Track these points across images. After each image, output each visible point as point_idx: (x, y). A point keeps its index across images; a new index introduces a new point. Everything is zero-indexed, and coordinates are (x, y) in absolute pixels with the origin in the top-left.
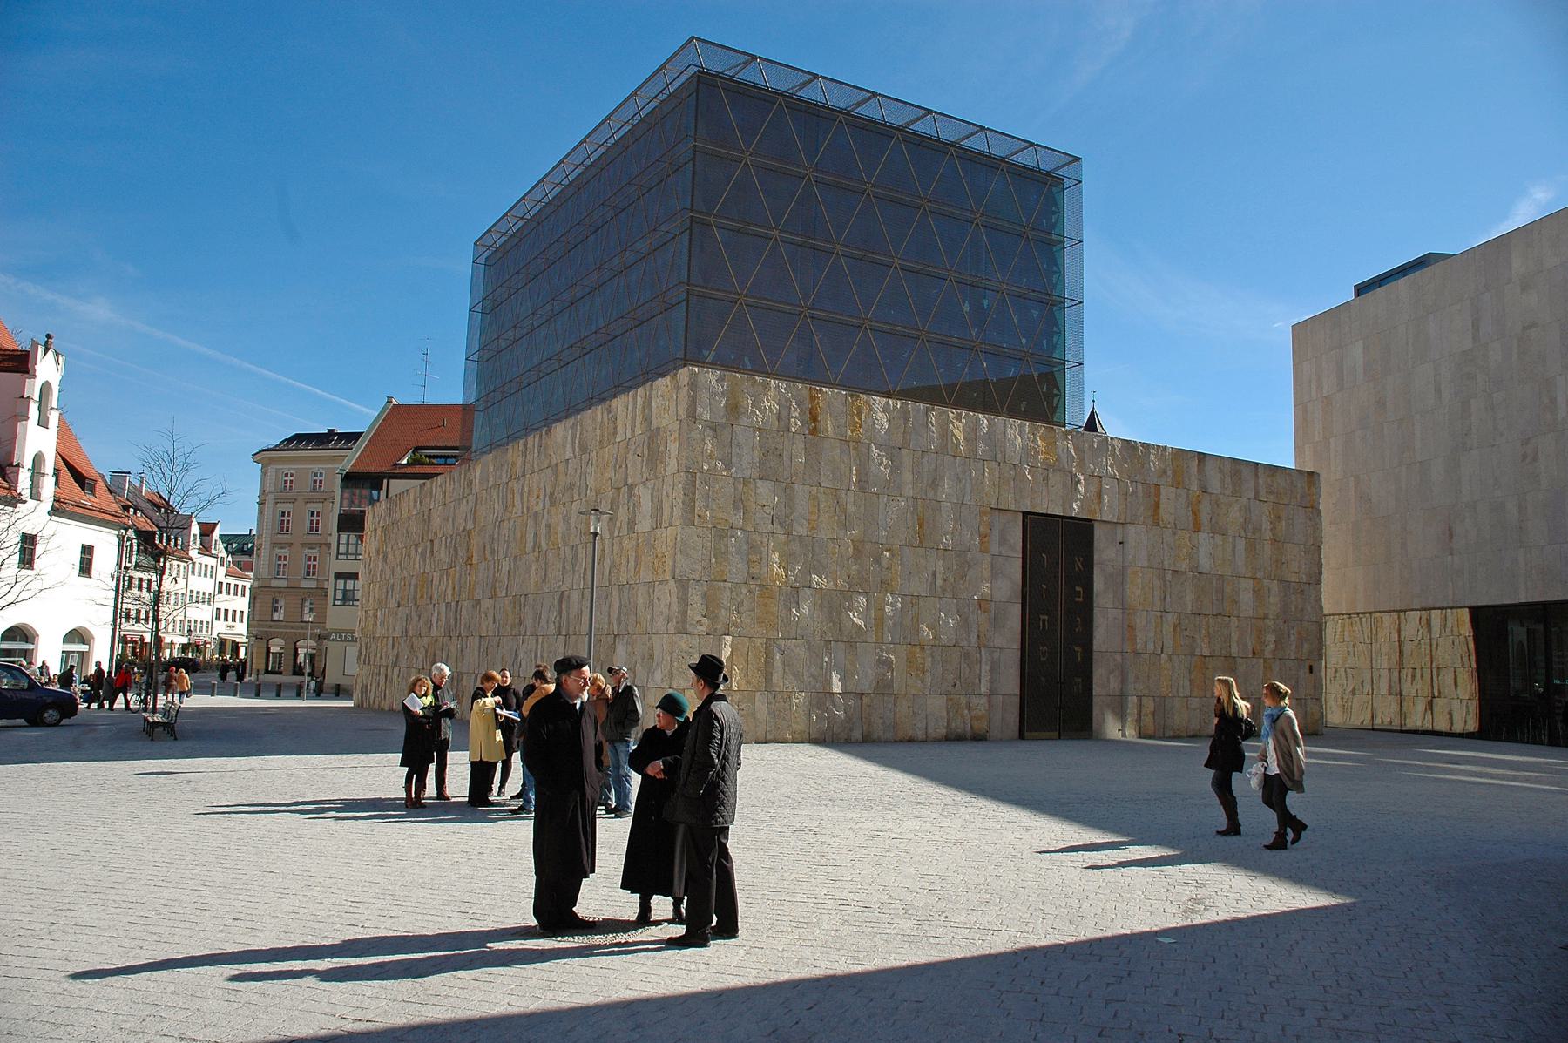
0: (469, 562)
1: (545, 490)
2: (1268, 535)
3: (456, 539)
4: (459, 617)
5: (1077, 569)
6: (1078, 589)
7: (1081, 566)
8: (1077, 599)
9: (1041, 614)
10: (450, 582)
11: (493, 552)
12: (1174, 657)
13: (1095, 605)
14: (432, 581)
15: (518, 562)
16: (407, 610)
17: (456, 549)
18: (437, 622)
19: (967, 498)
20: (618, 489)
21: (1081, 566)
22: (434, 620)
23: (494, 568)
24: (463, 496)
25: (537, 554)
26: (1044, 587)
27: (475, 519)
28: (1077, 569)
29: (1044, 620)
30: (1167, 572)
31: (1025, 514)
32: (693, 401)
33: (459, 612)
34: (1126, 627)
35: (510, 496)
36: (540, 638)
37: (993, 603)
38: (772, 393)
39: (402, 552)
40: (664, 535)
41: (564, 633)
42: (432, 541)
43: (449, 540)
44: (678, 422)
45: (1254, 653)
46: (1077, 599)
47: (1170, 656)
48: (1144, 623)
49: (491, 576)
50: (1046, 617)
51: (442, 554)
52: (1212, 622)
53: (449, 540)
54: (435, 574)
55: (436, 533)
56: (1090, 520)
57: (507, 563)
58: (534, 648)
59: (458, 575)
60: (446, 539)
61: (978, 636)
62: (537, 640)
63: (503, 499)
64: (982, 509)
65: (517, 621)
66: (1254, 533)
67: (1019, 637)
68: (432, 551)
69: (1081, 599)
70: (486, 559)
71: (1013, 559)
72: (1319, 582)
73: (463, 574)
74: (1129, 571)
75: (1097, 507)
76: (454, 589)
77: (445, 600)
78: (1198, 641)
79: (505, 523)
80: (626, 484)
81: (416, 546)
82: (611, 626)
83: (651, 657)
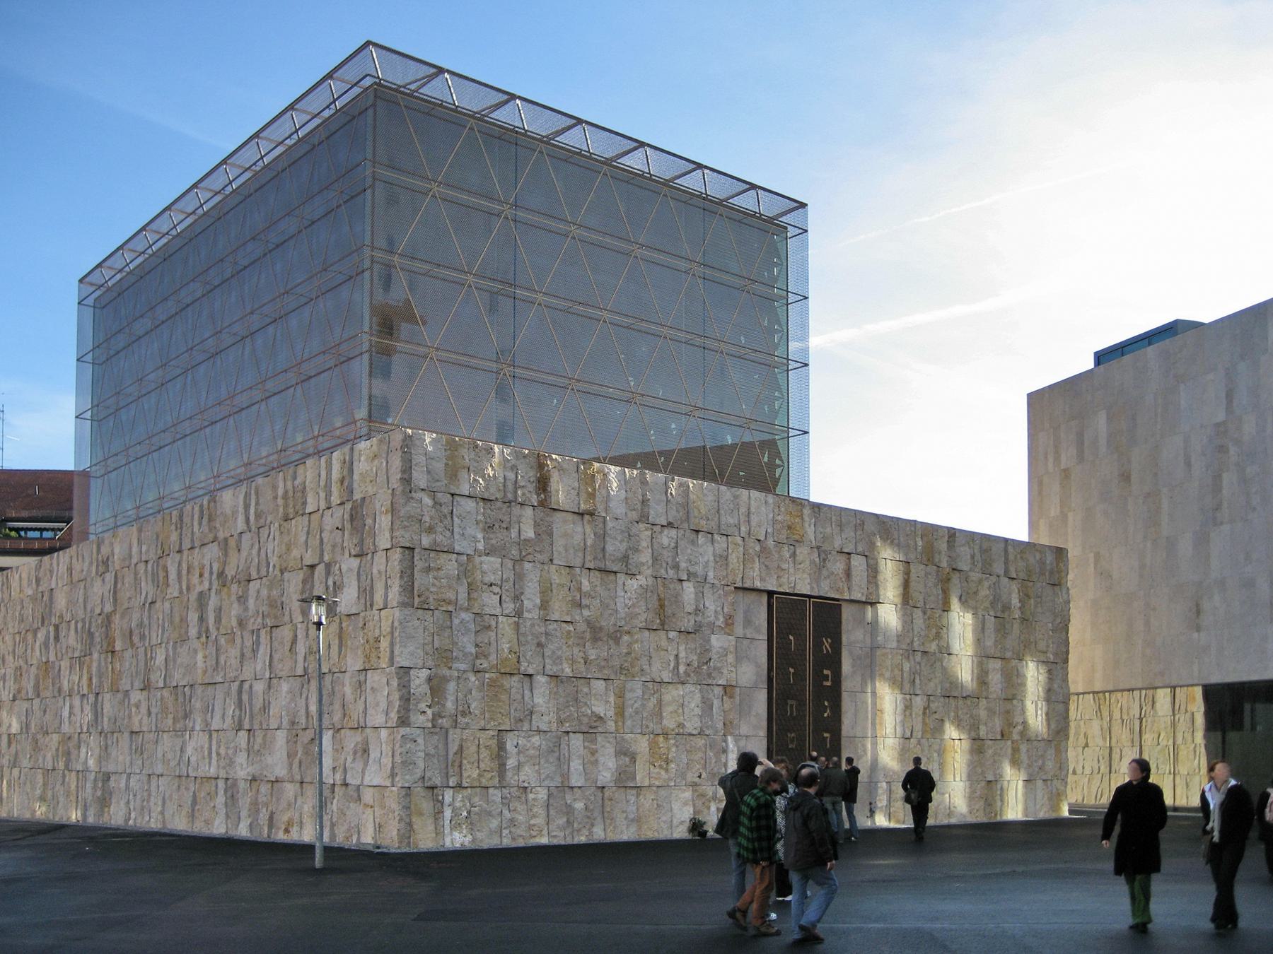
0: (110, 648)
1: (211, 568)
2: (1017, 614)
3: (90, 623)
4: (99, 710)
6: (826, 672)
7: (830, 650)
9: (788, 698)
10: (85, 672)
11: (143, 637)
12: (924, 741)
13: (843, 688)
14: (60, 670)
15: (179, 649)
16: (26, 705)
17: (91, 635)
18: (70, 717)
19: (711, 574)
20: (312, 567)
21: (830, 650)
22: (66, 713)
23: (146, 655)
24: (97, 573)
25: (203, 639)
26: (792, 670)
27: (115, 600)
31: (770, 594)
32: (407, 469)
33: (99, 704)
35: (162, 574)
36: (215, 735)
37: (738, 689)
38: (496, 460)
39: (14, 638)
40: (376, 618)
41: (247, 726)
42: (57, 627)
43: (80, 625)
44: (390, 491)
45: (1002, 736)
47: (919, 743)
49: (142, 664)
50: (794, 702)
51: (71, 639)
52: (961, 702)
53: (80, 625)
54: (63, 663)
55: (61, 617)
56: (837, 600)
57: (163, 650)
58: (207, 746)
59: (95, 665)
60: (77, 622)
62: (211, 736)
63: (153, 574)
64: (726, 588)
65: (181, 714)
66: (1003, 612)
67: (765, 724)
68: (57, 638)
69: (829, 683)
70: (133, 645)
71: (758, 642)
72: (1066, 661)
73: (103, 664)
74: (879, 653)
75: (845, 586)
76: (91, 679)
77: (79, 692)
79: (158, 605)
80: (321, 561)
81: (35, 632)
82: (310, 718)
83: (366, 751)
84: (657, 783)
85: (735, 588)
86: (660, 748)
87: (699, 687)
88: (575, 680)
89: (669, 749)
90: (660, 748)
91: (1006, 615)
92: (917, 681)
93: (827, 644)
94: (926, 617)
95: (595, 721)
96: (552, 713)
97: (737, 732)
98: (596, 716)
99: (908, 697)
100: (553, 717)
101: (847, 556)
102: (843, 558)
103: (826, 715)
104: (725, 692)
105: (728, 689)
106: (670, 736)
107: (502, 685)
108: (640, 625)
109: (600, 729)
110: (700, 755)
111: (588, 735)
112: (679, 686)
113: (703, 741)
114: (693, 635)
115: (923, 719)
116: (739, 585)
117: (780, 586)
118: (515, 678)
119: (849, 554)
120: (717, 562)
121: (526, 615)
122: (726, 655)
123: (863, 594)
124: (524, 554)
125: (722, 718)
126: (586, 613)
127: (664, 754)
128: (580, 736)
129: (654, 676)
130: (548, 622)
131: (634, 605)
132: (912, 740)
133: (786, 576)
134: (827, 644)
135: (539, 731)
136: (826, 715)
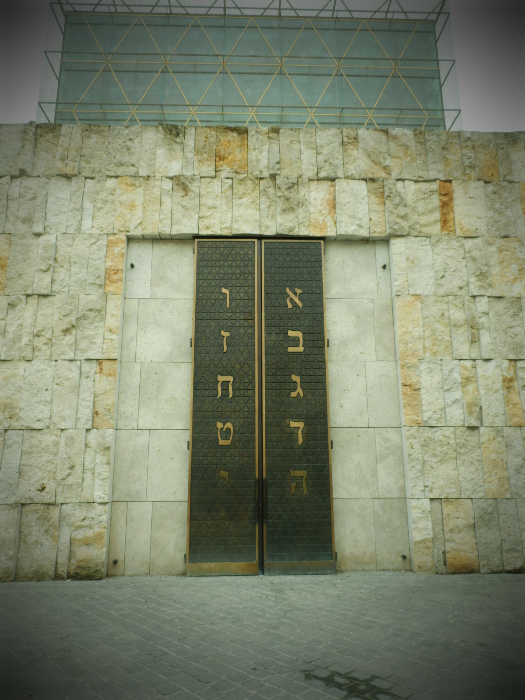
5: (290, 306)
6: (291, 333)
8: (291, 349)
26: (225, 334)
28: (290, 306)
29: (225, 384)
30: (478, 299)
34: (400, 386)
37: (137, 367)
46: (291, 349)
48: (437, 378)
50: (230, 379)
64: (111, 238)
69: (301, 349)
74: (398, 302)
75: (329, 217)
87: (54, 363)
92: (485, 338)
97: (134, 424)
99: (469, 364)
101: (329, 183)
103: (294, 394)
104: (101, 369)
105: (105, 364)
113: (54, 438)
115: (505, 397)
116: (138, 232)
117: (207, 228)
119: (333, 180)
120: (100, 209)
122: (103, 319)
123: (360, 226)
125: (88, 404)
132: (482, 430)
133: (218, 215)
136: (294, 394)
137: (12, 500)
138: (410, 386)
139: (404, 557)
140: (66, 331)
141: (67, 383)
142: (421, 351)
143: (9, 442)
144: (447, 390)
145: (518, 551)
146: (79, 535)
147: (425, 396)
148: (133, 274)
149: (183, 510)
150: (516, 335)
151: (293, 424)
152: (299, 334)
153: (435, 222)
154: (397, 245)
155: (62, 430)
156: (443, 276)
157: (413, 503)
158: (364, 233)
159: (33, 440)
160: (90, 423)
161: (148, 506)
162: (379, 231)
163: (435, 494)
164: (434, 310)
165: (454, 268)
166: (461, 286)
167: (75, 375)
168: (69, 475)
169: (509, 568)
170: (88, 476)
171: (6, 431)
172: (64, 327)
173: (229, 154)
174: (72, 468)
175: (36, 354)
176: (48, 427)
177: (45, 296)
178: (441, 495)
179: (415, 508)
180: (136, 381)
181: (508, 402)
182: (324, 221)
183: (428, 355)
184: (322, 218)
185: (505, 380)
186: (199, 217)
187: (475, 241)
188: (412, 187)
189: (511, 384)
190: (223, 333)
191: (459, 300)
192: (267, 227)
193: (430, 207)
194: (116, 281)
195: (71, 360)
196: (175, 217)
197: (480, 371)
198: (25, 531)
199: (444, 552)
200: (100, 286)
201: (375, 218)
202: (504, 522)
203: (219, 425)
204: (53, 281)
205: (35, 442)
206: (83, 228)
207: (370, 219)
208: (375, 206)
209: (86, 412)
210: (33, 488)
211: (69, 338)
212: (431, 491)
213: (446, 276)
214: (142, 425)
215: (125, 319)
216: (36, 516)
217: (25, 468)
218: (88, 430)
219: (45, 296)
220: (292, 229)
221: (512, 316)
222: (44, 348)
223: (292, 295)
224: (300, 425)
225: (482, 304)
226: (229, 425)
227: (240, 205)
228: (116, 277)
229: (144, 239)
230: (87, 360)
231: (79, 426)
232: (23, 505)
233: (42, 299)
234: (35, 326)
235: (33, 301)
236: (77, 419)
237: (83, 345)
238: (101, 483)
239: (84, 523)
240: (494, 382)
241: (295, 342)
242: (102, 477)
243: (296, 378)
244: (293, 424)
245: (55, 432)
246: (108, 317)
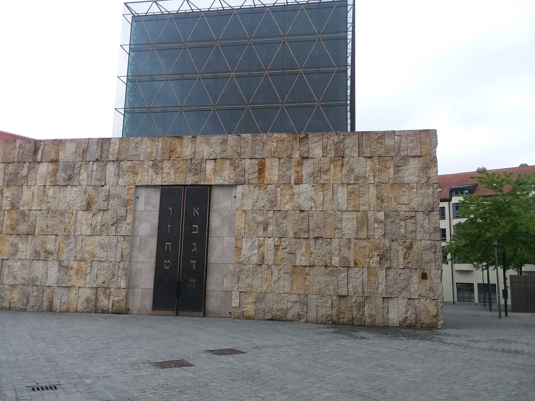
6: (194, 226)
8: (193, 232)
29: (168, 246)
30: (269, 211)
46: (193, 232)
50: (170, 244)
61: (122, 256)
69: (197, 232)
78: (299, 256)
84: (79, 285)
85: (136, 186)
86: (82, 267)
87: (108, 237)
88: (41, 235)
89: (86, 268)
90: (82, 267)
91: (361, 182)
93: (196, 211)
94: (279, 189)
95: (48, 255)
96: (28, 251)
98: (48, 252)
100: (29, 253)
102: (212, 162)
103: (193, 250)
105: (126, 237)
106: (87, 262)
107: (6, 240)
108: (77, 209)
109: (50, 259)
110: (106, 271)
111: (45, 261)
112: (98, 237)
113: (108, 264)
114: (107, 211)
116: (140, 184)
118: (13, 236)
121: (21, 208)
123: (224, 180)
124: (23, 182)
126: (50, 205)
127: (84, 270)
128: (42, 262)
129: (82, 232)
130: (32, 211)
131: (74, 199)
134: (196, 211)
135: (20, 259)
136: (193, 250)
137: (94, 286)
138: (238, 247)
139: (230, 313)
140: (112, 225)
141: (112, 244)
142: (243, 234)
143: (93, 265)
144: (252, 250)
145: (270, 313)
146: (116, 299)
147: (243, 252)
148: (138, 201)
149: (152, 291)
150: (283, 227)
151: (192, 262)
152: (197, 226)
153: (256, 178)
154: (239, 188)
155: (111, 262)
156: (257, 202)
157: (233, 293)
158: (226, 183)
159: (101, 265)
160: (120, 259)
161: (141, 290)
162: (232, 182)
163: (242, 290)
164: (250, 217)
165: (261, 198)
166: (263, 206)
167: (116, 241)
168: (113, 278)
169: (266, 319)
170: (119, 278)
171: (92, 261)
172: (112, 223)
173: (175, 149)
174: (114, 275)
175: (102, 233)
176: (106, 261)
177: (106, 210)
178: (244, 290)
179: (233, 294)
180: (138, 243)
181: (275, 255)
182: (211, 178)
183: (246, 235)
184: (210, 177)
185: (275, 246)
186: (162, 178)
187: (272, 185)
188: (248, 162)
189: (278, 248)
190: (168, 225)
191: (262, 212)
192: (188, 181)
193: (254, 171)
194: (131, 204)
195: (114, 236)
196: (153, 177)
197: (266, 242)
198: (98, 297)
199: (243, 312)
200: (125, 207)
201: (231, 176)
202: (267, 301)
203: (165, 261)
204: (108, 205)
205: (102, 265)
206: (119, 183)
207: (229, 177)
208: (232, 171)
209: (119, 256)
210: (101, 282)
211: (114, 228)
212: (241, 289)
213: (258, 201)
214: (139, 260)
215: (134, 219)
216: (102, 292)
217: (98, 275)
218: (119, 262)
219: (106, 210)
220: (198, 182)
221: (282, 219)
222: (105, 231)
223: (196, 210)
224: (195, 262)
225: (271, 214)
226: (169, 261)
227: (177, 172)
228: (131, 203)
229: (142, 186)
230: (119, 235)
231: (117, 260)
232: (98, 288)
233: (104, 211)
234: (102, 222)
235: (101, 212)
236: (116, 258)
237: (118, 229)
238: (123, 281)
239: (117, 295)
240: (270, 247)
241: (195, 229)
242: (124, 279)
243: (194, 244)
244: (192, 262)
245: (109, 262)
246: (127, 219)
